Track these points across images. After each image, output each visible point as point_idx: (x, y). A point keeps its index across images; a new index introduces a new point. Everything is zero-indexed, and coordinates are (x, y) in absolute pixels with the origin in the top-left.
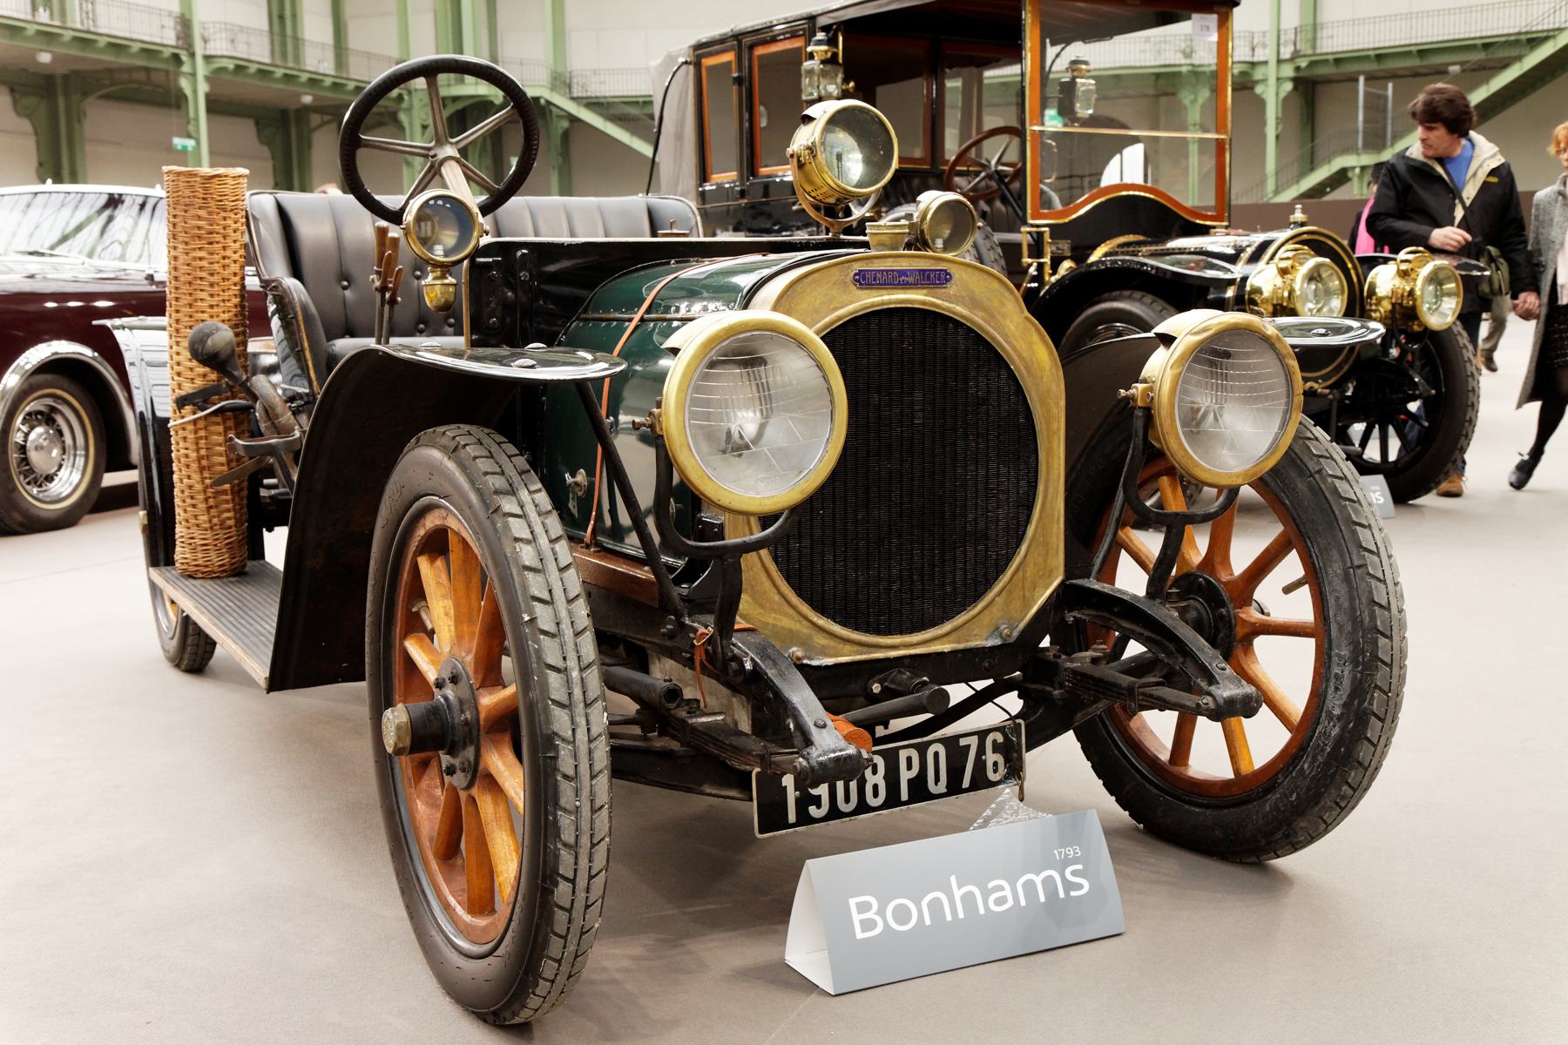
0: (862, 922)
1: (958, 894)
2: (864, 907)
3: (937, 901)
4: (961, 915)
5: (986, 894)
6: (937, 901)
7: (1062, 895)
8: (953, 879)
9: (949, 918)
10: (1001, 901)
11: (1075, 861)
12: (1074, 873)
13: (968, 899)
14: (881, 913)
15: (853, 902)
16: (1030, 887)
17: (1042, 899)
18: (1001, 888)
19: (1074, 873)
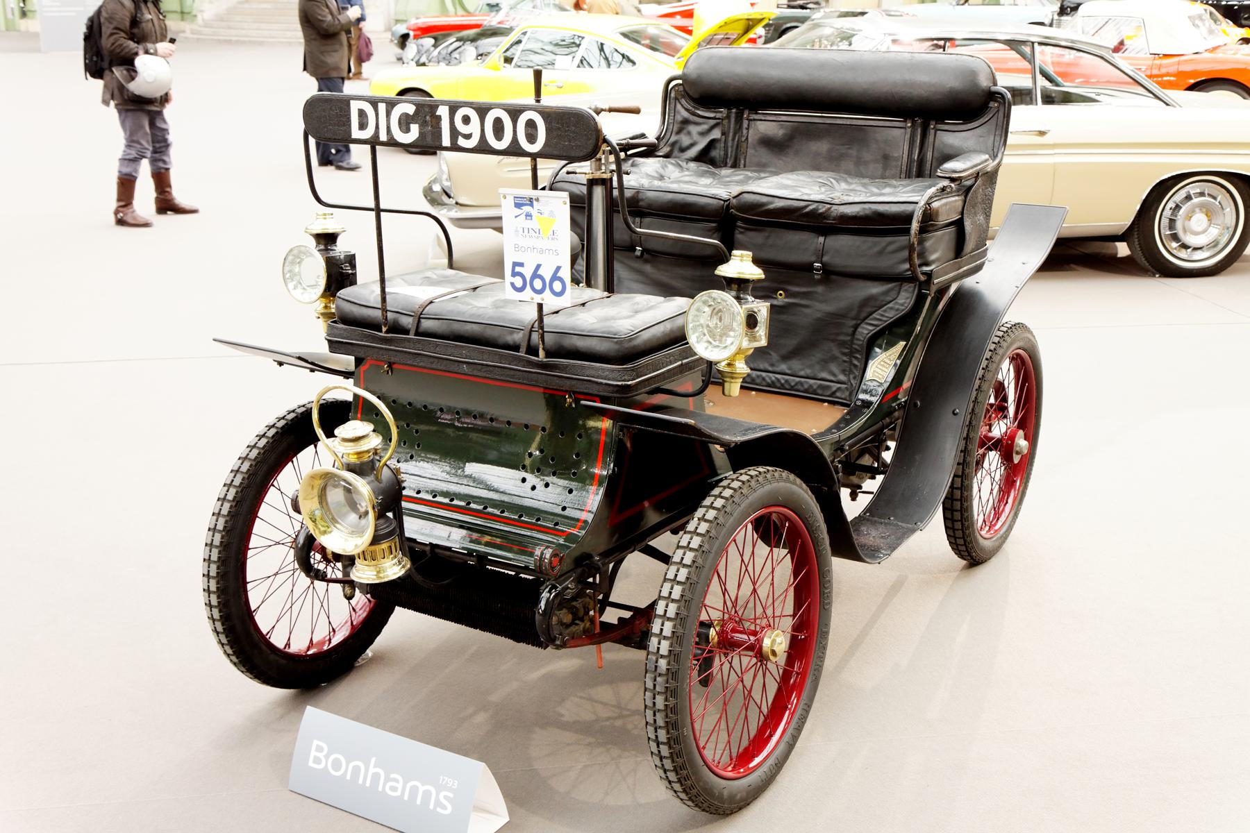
1: (372, 770)
2: (319, 749)
3: (356, 770)
4: (368, 784)
5: (387, 780)
7: (431, 807)
9: (360, 782)
10: (394, 789)
11: (450, 790)
12: (446, 797)
13: (376, 777)
14: (327, 757)
15: (316, 743)
16: (414, 790)
17: (418, 802)
19: (446, 797)
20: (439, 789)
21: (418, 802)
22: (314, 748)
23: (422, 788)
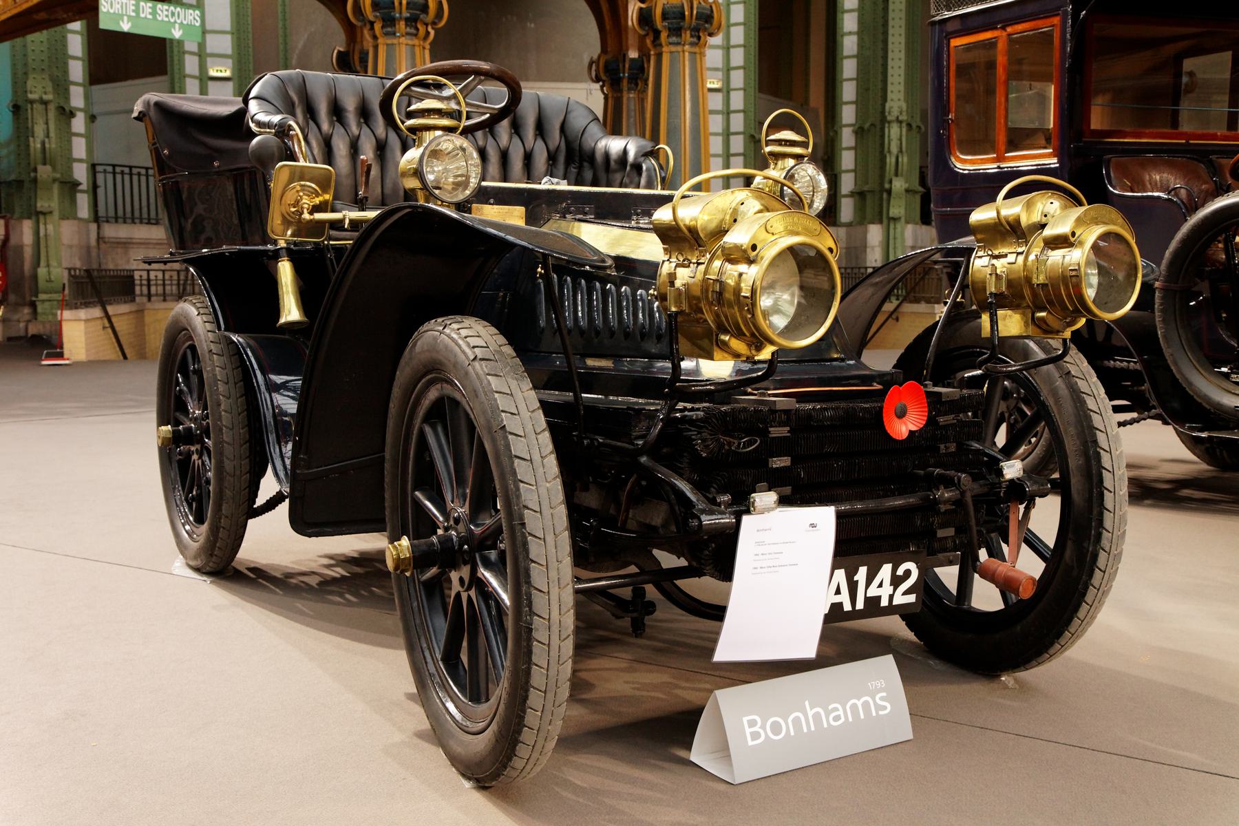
0: (752, 733)
1: (810, 713)
3: (797, 722)
4: (813, 729)
5: (828, 714)
8: (807, 703)
9: (805, 730)
10: (837, 718)
11: (881, 690)
12: (882, 699)
13: (817, 717)
14: (763, 727)
15: (745, 719)
16: (854, 707)
18: (836, 709)
19: (882, 699)
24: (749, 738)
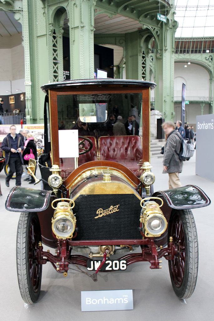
1: (105, 300)
3: (100, 301)
4: (104, 303)
6: (101, 300)
7: (123, 302)
9: (102, 303)
10: (111, 302)
11: (126, 297)
12: (126, 299)
13: (106, 301)
16: (117, 301)
17: (119, 303)
19: (126, 299)
20: (123, 298)
21: (119, 303)
22: (87, 300)
23: (119, 300)
24: (87, 302)
